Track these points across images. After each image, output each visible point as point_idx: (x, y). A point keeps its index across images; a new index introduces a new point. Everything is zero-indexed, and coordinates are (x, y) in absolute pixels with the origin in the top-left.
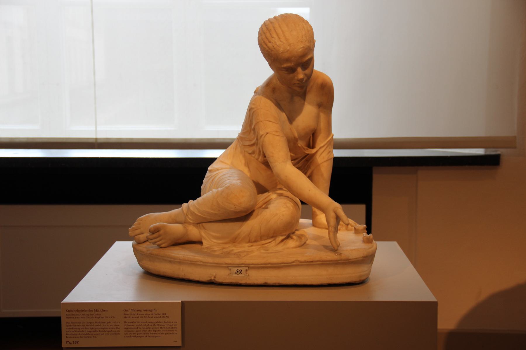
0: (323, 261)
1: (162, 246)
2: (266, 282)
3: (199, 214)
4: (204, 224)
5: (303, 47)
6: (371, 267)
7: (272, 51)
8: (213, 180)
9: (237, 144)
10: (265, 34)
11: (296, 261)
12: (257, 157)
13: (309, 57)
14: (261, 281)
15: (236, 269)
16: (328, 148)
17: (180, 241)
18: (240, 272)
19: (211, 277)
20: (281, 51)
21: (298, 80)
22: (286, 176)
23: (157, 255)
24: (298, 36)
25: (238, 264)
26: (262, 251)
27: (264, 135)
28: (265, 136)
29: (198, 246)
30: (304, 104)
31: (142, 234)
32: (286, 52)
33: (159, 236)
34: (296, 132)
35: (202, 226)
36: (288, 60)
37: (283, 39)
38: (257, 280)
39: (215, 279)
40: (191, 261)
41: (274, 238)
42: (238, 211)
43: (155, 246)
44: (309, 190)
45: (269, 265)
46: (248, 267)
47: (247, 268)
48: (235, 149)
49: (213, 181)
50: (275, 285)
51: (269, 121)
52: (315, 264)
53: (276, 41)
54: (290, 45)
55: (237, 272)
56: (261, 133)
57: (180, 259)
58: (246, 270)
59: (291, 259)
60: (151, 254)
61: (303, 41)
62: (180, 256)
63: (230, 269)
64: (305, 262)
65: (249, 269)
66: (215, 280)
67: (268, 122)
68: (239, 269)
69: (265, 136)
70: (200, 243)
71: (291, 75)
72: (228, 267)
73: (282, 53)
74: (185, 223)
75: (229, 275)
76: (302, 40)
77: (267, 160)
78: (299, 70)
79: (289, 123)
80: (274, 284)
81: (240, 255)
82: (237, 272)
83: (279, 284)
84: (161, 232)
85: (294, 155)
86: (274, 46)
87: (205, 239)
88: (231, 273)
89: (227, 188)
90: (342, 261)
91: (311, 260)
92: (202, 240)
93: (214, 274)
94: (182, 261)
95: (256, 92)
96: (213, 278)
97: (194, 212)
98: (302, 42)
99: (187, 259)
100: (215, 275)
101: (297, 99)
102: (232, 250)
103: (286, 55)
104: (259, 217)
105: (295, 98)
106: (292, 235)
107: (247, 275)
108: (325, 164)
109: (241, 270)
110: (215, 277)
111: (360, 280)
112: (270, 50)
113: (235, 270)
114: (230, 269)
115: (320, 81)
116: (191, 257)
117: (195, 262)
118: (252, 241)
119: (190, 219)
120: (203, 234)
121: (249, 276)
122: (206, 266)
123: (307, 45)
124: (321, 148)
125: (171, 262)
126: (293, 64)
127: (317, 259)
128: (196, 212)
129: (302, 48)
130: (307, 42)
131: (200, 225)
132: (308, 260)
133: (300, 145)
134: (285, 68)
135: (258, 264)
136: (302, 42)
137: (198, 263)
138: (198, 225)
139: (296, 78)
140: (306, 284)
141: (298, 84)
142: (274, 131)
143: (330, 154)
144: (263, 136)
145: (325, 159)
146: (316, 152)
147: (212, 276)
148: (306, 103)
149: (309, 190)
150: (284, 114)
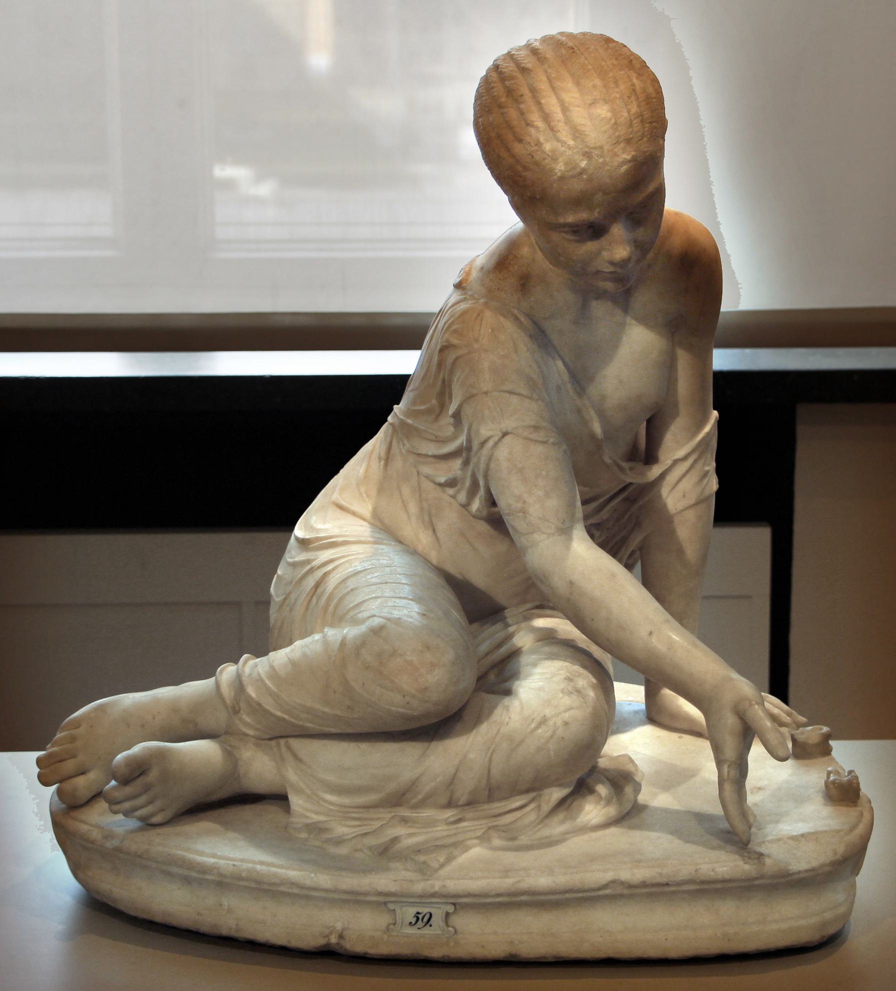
0: (703, 882)
1: (155, 820)
2: (514, 952)
3: (279, 714)
4: (292, 741)
5: (634, 159)
6: (853, 886)
7: (526, 168)
8: (317, 585)
9: (391, 443)
10: (502, 111)
11: (614, 882)
12: (462, 497)
13: (651, 188)
14: (497, 949)
15: (411, 912)
16: (701, 463)
17: (214, 797)
18: (426, 919)
19: (327, 936)
20: (559, 174)
21: (612, 263)
22: (571, 583)
23: (140, 856)
24: (616, 123)
25: (421, 896)
26: (497, 842)
27: (496, 439)
28: (496, 444)
29: (271, 812)
31: (83, 773)
32: (573, 177)
33: (147, 788)
35: (289, 748)
36: (579, 201)
37: (564, 134)
38: (483, 946)
39: (343, 942)
40: (257, 882)
41: (532, 795)
42: (415, 714)
43: (132, 823)
44: (651, 633)
45: (524, 898)
46: (454, 904)
47: (451, 909)
48: (382, 463)
49: (319, 590)
50: (543, 960)
51: (511, 392)
52: (674, 892)
53: (542, 139)
54: (587, 155)
55: (414, 921)
56: (485, 432)
57: (221, 875)
58: (447, 915)
59: (598, 875)
60: (118, 850)
61: (632, 138)
62: (222, 862)
63: (394, 910)
64: (644, 884)
65: (455, 908)
66: (341, 947)
67: (507, 395)
68: (424, 910)
69: (496, 444)
70: (280, 799)
71: (591, 246)
72: (385, 903)
73: (562, 179)
74: (226, 733)
75: (388, 928)
76: (631, 136)
77: (499, 512)
78: (618, 230)
80: (538, 958)
81: (424, 862)
82: (415, 919)
83: (555, 957)
84: (153, 775)
85: (587, 489)
86: (534, 155)
87: (299, 791)
88: (394, 924)
89: (377, 631)
90: (769, 881)
91: (664, 880)
92: (287, 793)
93: (339, 926)
94: (228, 880)
95: (464, 285)
96: (334, 940)
97: (259, 705)
99: (244, 875)
100: (343, 930)
101: (599, 309)
102: (396, 840)
103: (577, 186)
104: (484, 727)
105: (594, 303)
106: (590, 781)
107: (451, 929)
108: (691, 515)
109: (431, 915)
110: (341, 936)
111: (823, 937)
112: (520, 168)
113: (410, 913)
114: (394, 910)
116: (258, 867)
117: (274, 884)
118: (460, 803)
119: (247, 722)
120: (292, 775)
121: (456, 932)
122: (308, 898)
123: (645, 152)
124: (676, 462)
125: (187, 881)
126: (596, 214)
127: (685, 872)
128: (269, 704)
129: (629, 161)
131: (278, 745)
132: (654, 881)
133: (608, 461)
134: (570, 225)
135: (486, 895)
137: (282, 889)
138: (273, 743)
139: (605, 254)
140: (645, 956)
141: (611, 273)
142: (529, 427)
143: (705, 481)
144: (491, 443)
145: (692, 502)
146: (662, 476)
147: (331, 933)
149: (651, 633)
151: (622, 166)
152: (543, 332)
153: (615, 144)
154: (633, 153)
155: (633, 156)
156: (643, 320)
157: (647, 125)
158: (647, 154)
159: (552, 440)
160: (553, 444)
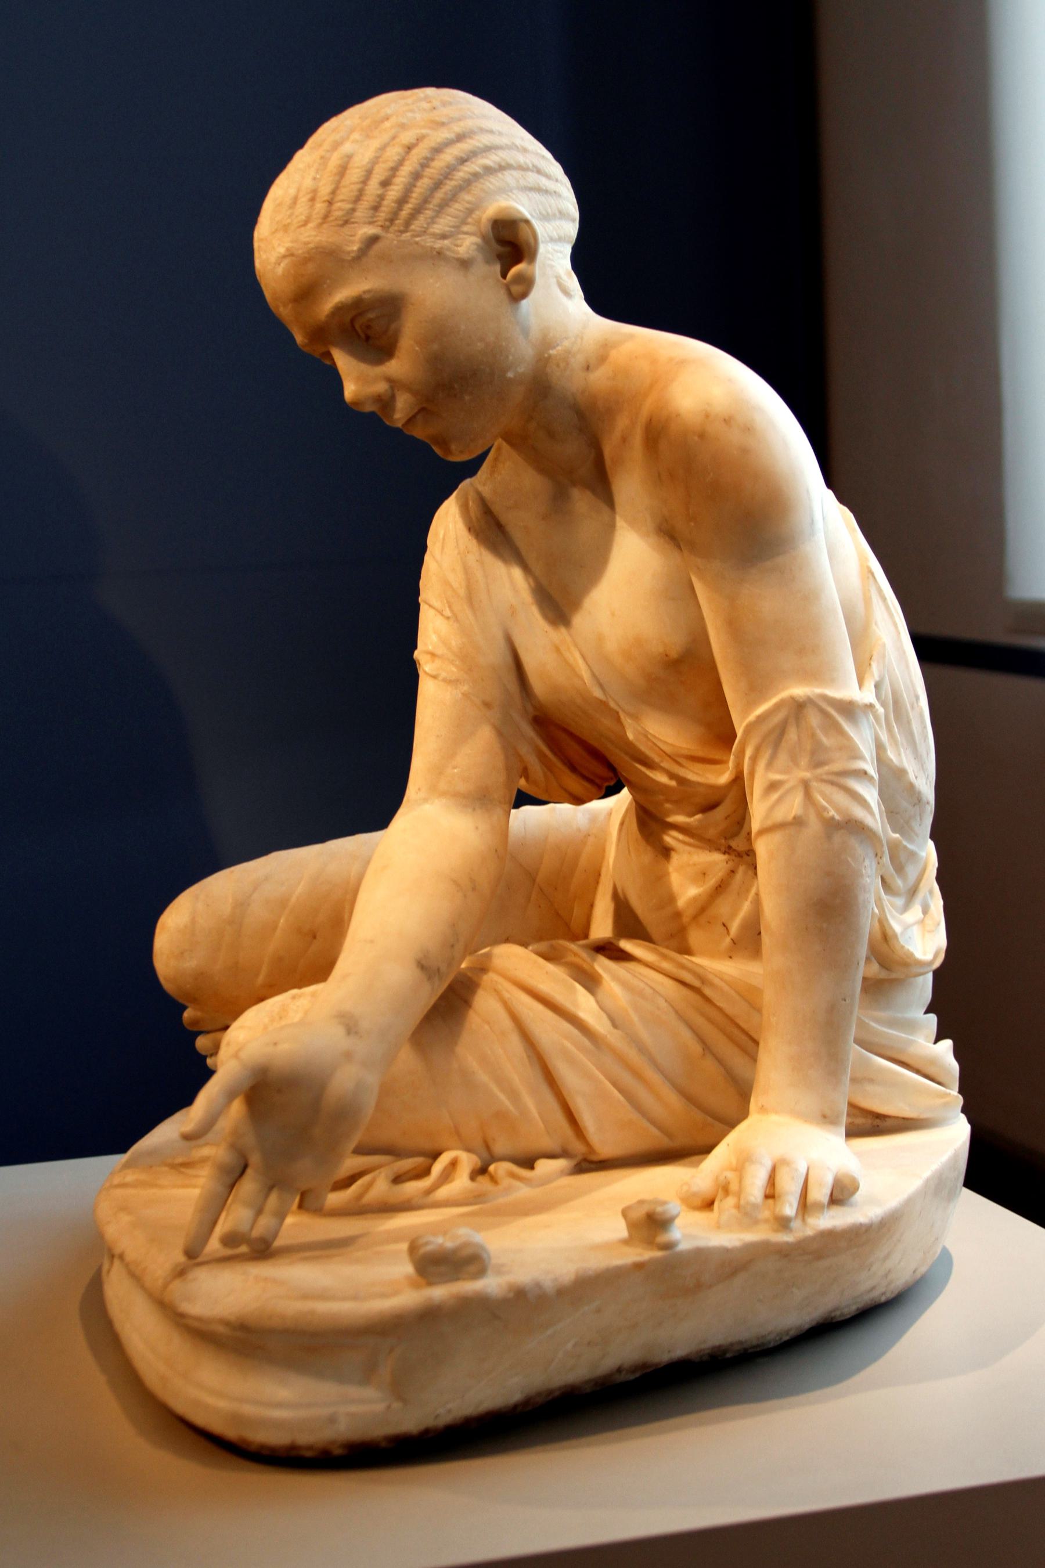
5: (290, 254)
30: (611, 527)
76: (289, 221)
79: (546, 617)
85: (673, 783)
98: (286, 228)
101: (581, 500)
105: (576, 493)
115: (647, 408)
123: (308, 243)
129: (284, 257)
130: (310, 225)
136: (286, 228)
143: (775, 796)
148: (620, 522)
150: (517, 573)
151: (279, 264)
152: (500, 527)
154: (288, 245)
155: (288, 249)
159: (444, 674)
160: (444, 680)
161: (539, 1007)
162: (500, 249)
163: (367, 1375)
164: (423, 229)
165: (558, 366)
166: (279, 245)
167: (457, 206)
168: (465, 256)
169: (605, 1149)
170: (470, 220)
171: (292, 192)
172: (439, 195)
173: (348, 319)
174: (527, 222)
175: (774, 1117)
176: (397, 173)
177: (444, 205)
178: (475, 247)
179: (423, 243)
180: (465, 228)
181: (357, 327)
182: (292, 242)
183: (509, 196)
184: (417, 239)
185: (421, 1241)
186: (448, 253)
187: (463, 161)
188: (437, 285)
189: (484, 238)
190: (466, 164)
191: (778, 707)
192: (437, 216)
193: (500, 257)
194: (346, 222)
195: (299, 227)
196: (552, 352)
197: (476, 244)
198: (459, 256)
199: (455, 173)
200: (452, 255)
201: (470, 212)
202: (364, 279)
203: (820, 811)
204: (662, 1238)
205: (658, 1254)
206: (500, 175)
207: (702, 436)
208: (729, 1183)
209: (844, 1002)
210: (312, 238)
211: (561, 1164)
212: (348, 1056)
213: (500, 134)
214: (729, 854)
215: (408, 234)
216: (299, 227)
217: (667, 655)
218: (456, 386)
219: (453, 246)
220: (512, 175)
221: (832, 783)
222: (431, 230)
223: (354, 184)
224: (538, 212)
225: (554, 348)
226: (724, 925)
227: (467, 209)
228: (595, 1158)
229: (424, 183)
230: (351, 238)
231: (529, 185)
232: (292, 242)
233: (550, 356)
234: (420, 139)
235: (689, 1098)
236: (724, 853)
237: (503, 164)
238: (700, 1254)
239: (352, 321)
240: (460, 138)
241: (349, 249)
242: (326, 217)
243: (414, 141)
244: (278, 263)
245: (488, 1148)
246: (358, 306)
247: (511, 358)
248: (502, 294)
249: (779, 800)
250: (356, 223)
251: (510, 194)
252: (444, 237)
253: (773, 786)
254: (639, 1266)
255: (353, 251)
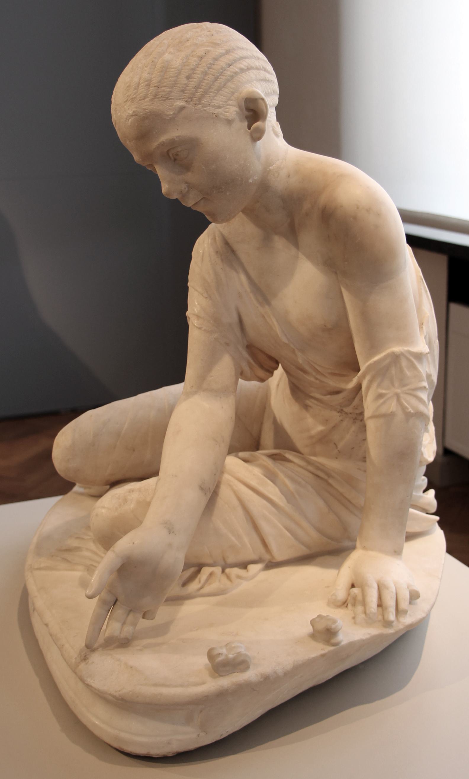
5: (135, 114)
16: (374, 385)
34: (275, 323)
76: (134, 96)
98: (133, 100)
105: (276, 238)
123: (144, 109)
129: (132, 116)
136: (133, 100)
143: (381, 401)
151: (129, 120)
152: (233, 251)
153: (125, 102)
154: (134, 109)
155: (134, 112)
156: (309, 257)
157: (152, 88)
158: (146, 111)
159: (204, 328)
160: (205, 330)
161: (250, 492)
162: (247, 113)
163: (189, 720)
164: (209, 103)
165: (274, 175)
166: (129, 109)
167: (226, 90)
168: (230, 118)
169: (279, 557)
170: (232, 98)
171: (136, 80)
172: (217, 84)
173: (166, 150)
174: (263, 99)
175: (371, 553)
176: (195, 72)
177: (219, 90)
178: (235, 112)
179: (208, 110)
180: (230, 102)
181: (171, 155)
182: (136, 108)
183: (252, 84)
184: (205, 108)
185: (216, 652)
186: (221, 116)
187: (229, 65)
188: (215, 134)
189: (240, 107)
190: (231, 67)
191: (386, 357)
192: (215, 96)
193: (247, 117)
194: (167, 98)
195: (140, 100)
196: (271, 168)
197: (235, 111)
198: (227, 118)
199: (225, 72)
200: (224, 117)
201: (233, 93)
202: (176, 130)
203: (404, 409)
204: (334, 641)
205: (332, 648)
206: (247, 73)
207: (355, 218)
208: (357, 596)
209: (407, 498)
210: (147, 107)
211: (259, 566)
212: (170, 545)
213: (247, 50)
214: (341, 412)
215: (200, 106)
216: (140, 100)
217: (325, 326)
218: (223, 187)
219: (224, 112)
220: (253, 72)
221: (411, 394)
222: (212, 104)
223: (172, 77)
224: (265, 93)
225: (272, 165)
226: (335, 444)
227: (231, 92)
228: (274, 561)
229: (210, 77)
230: (170, 107)
231: (261, 78)
232: (136, 108)
233: (270, 170)
234: (207, 52)
235: (319, 531)
236: (339, 412)
237: (249, 67)
238: (351, 644)
239: (168, 151)
240: (228, 52)
241: (169, 113)
242: (155, 96)
243: (204, 54)
244: (127, 119)
245: (224, 559)
246: (173, 144)
247: (251, 172)
248: (248, 138)
249: (384, 403)
250: (173, 99)
251: (252, 83)
252: (219, 107)
253: (380, 396)
254: (323, 656)
255: (171, 115)
